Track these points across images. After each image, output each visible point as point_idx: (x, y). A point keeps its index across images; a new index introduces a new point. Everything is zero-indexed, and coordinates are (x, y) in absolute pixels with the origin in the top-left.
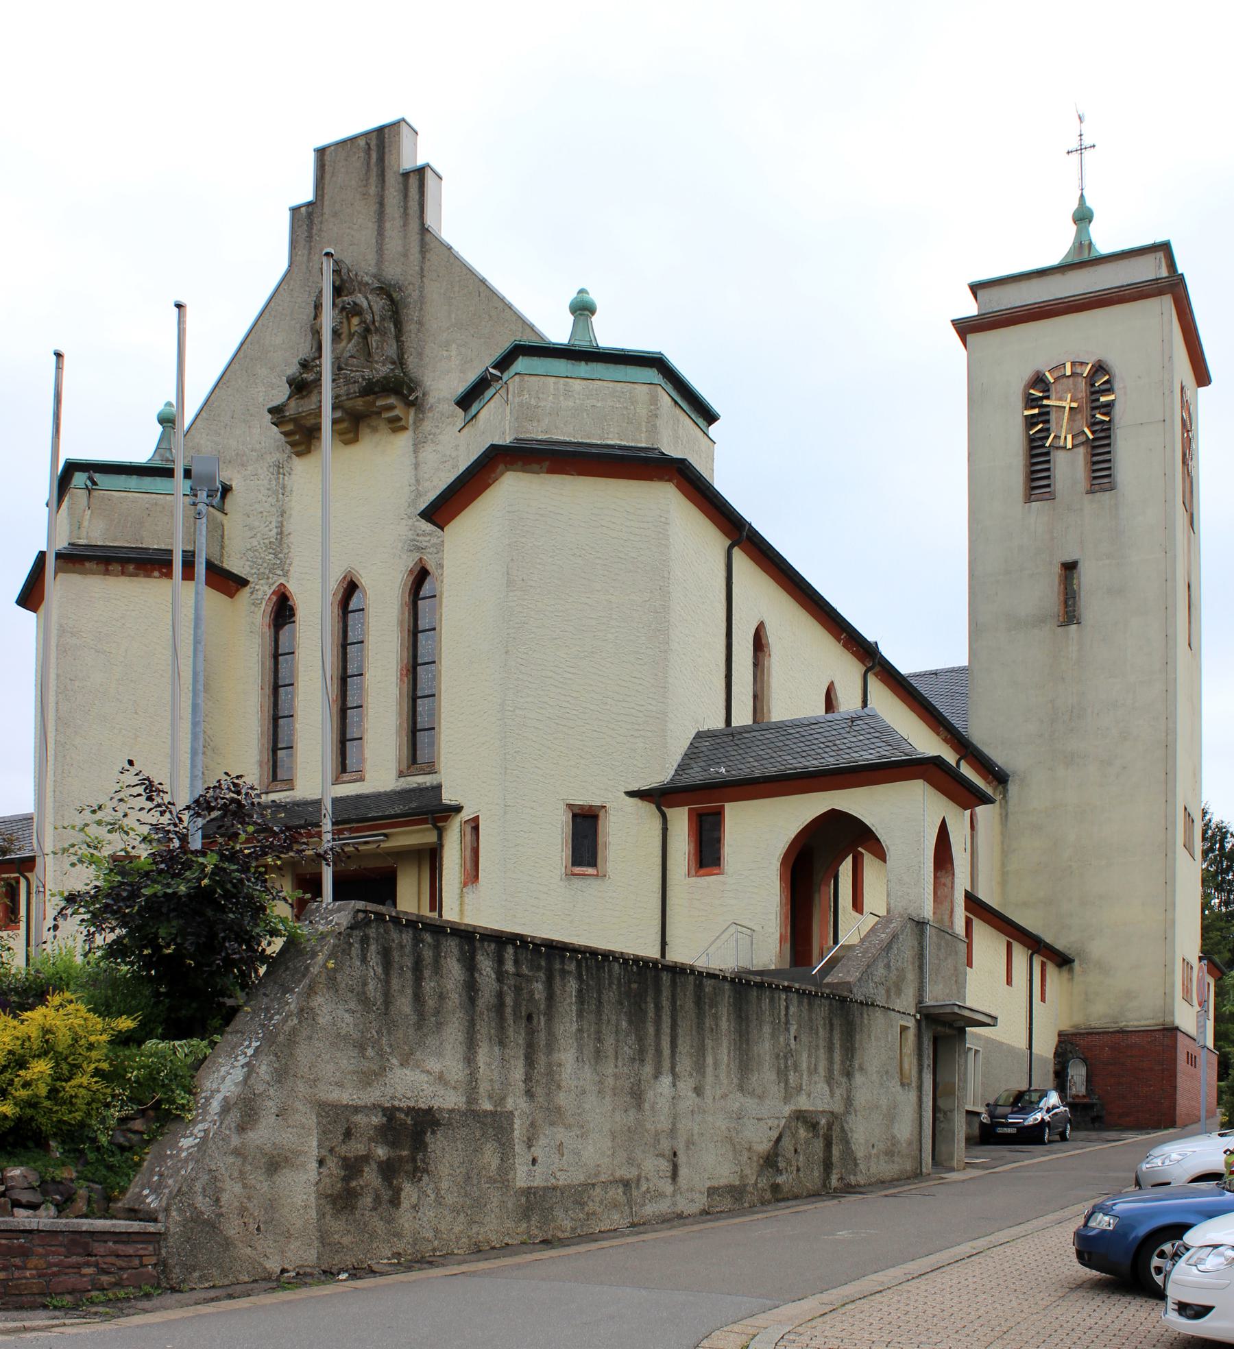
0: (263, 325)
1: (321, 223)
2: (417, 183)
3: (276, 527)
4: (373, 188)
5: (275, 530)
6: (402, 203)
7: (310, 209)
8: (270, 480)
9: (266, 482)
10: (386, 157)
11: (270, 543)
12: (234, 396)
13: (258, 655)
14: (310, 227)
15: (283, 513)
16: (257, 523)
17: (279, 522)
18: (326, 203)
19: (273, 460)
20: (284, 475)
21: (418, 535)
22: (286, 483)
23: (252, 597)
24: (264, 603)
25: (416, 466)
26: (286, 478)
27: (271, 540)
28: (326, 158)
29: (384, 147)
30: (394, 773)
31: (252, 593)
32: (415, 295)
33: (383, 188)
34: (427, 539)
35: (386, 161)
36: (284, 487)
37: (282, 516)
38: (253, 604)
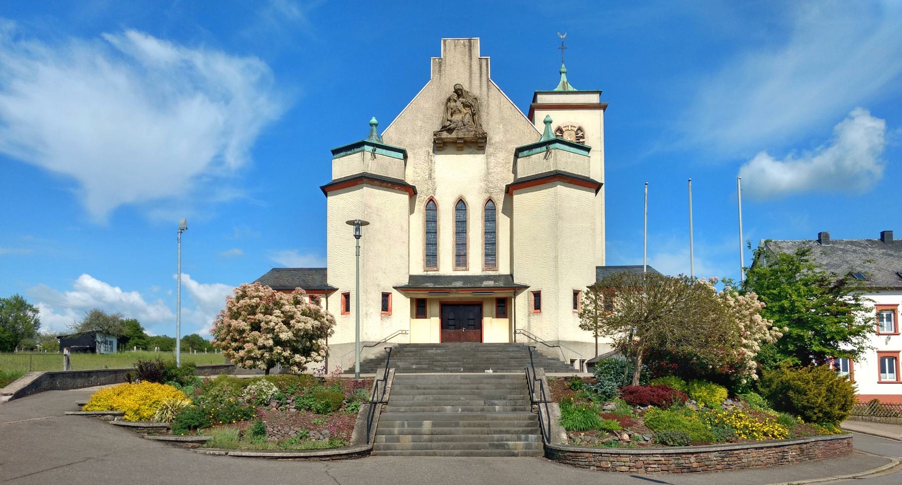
1: (445, 66)
4: (467, 60)
7: (440, 60)
8: (425, 157)
9: (423, 157)
10: (472, 50)
14: (440, 66)
16: (420, 172)
25: (487, 164)
30: (480, 270)
32: (485, 103)
33: (471, 61)
36: (431, 161)
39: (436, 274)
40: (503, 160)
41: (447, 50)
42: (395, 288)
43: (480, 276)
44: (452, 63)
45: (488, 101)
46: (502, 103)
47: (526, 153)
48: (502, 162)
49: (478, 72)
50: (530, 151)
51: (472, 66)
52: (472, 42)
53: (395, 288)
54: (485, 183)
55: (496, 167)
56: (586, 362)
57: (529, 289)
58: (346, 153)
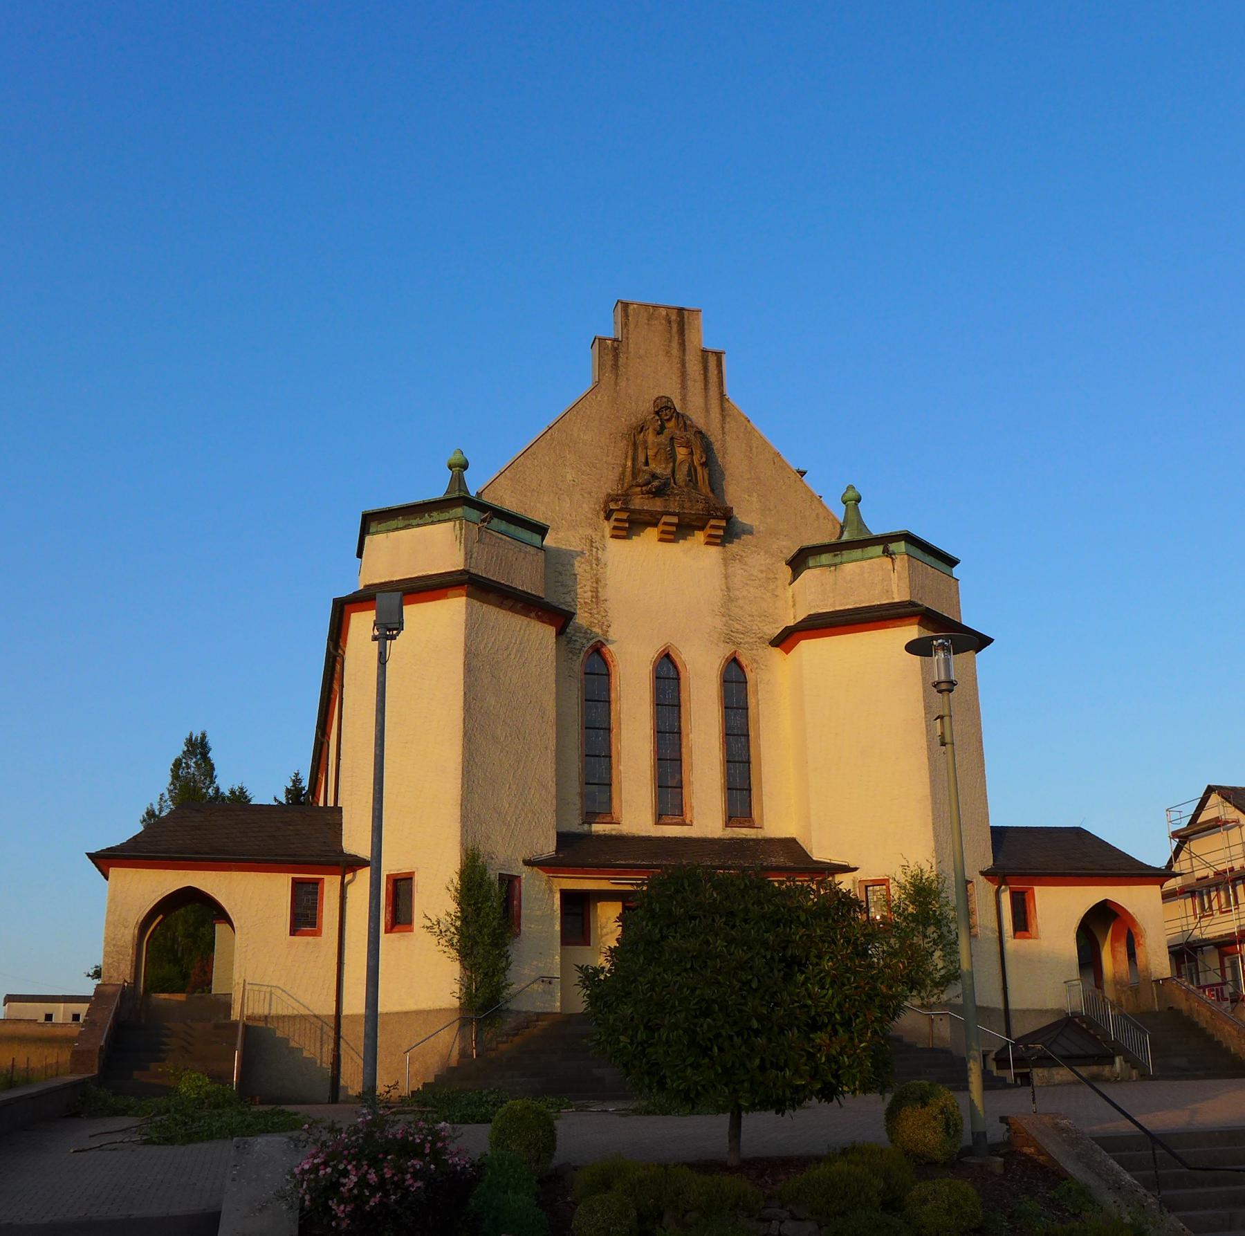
0: (570, 419)
2: (715, 362)
3: (592, 591)
4: (675, 350)
5: (589, 594)
6: (702, 372)
7: (616, 344)
10: (686, 332)
11: (585, 603)
12: (541, 469)
13: (578, 698)
14: (616, 357)
15: (597, 581)
17: (594, 587)
18: (631, 346)
19: (585, 534)
20: (598, 549)
21: (732, 631)
22: (600, 556)
23: (570, 646)
24: (582, 654)
25: (726, 577)
26: (599, 552)
27: (586, 600)
28: (629, 311)
29: (683, 325)
31: (569, 642)
34: (742, 636)
35: (686, 336)
36: (598, 559)
37: (597, 583)
38: (571, 652)
39: (614, 833)
40: (762, 572)
41: (632, 326)
42: (528, 863)
43: (720, 840)
44: (642, 352)
45: (724, 441)
46: (754, 449)
47: (825, 558)
48: (760, 575)
49: (700, 378)
50: (836, 555)
51: (687, 365)
52: (686, 317)
53: (528, 863)
54: (724, 619)
55: (748, 588)
56: (992, 1055)
57: (854, 873)
58: (407, 522)
